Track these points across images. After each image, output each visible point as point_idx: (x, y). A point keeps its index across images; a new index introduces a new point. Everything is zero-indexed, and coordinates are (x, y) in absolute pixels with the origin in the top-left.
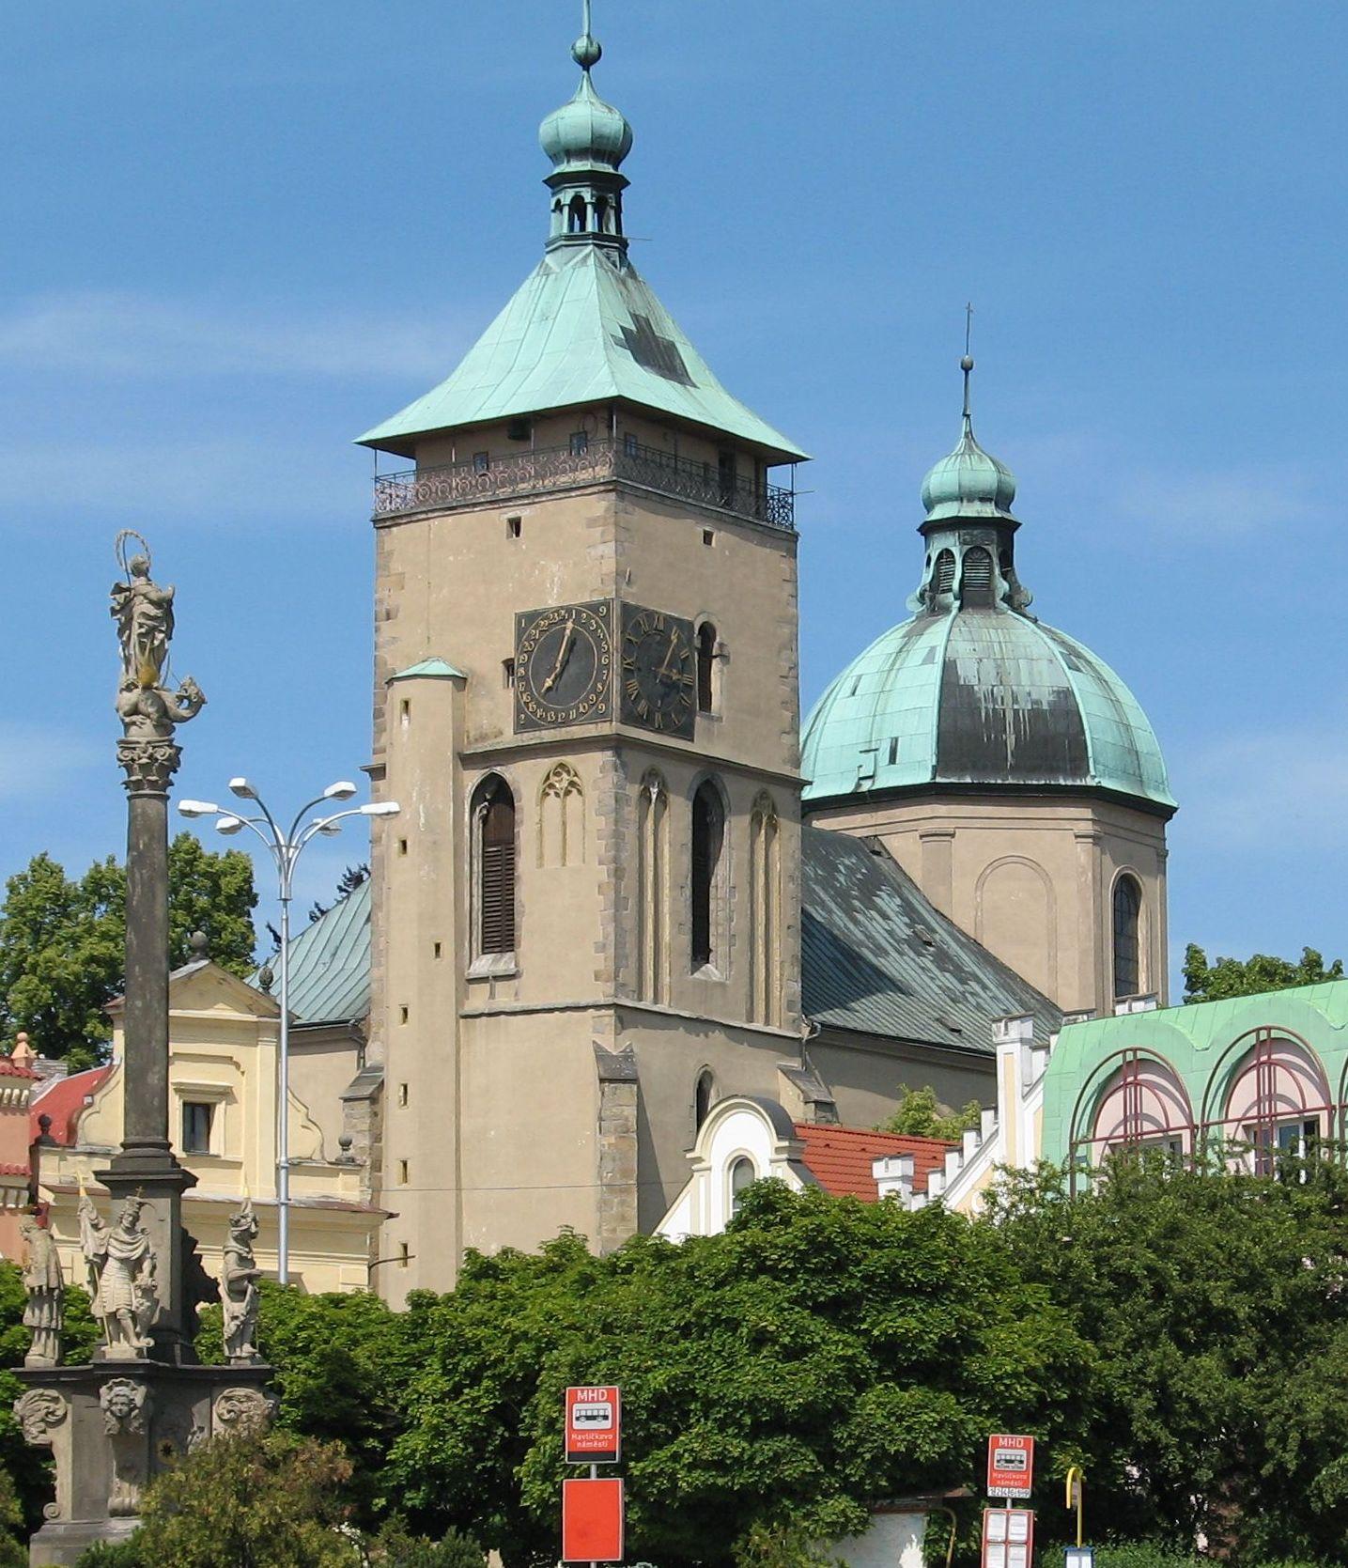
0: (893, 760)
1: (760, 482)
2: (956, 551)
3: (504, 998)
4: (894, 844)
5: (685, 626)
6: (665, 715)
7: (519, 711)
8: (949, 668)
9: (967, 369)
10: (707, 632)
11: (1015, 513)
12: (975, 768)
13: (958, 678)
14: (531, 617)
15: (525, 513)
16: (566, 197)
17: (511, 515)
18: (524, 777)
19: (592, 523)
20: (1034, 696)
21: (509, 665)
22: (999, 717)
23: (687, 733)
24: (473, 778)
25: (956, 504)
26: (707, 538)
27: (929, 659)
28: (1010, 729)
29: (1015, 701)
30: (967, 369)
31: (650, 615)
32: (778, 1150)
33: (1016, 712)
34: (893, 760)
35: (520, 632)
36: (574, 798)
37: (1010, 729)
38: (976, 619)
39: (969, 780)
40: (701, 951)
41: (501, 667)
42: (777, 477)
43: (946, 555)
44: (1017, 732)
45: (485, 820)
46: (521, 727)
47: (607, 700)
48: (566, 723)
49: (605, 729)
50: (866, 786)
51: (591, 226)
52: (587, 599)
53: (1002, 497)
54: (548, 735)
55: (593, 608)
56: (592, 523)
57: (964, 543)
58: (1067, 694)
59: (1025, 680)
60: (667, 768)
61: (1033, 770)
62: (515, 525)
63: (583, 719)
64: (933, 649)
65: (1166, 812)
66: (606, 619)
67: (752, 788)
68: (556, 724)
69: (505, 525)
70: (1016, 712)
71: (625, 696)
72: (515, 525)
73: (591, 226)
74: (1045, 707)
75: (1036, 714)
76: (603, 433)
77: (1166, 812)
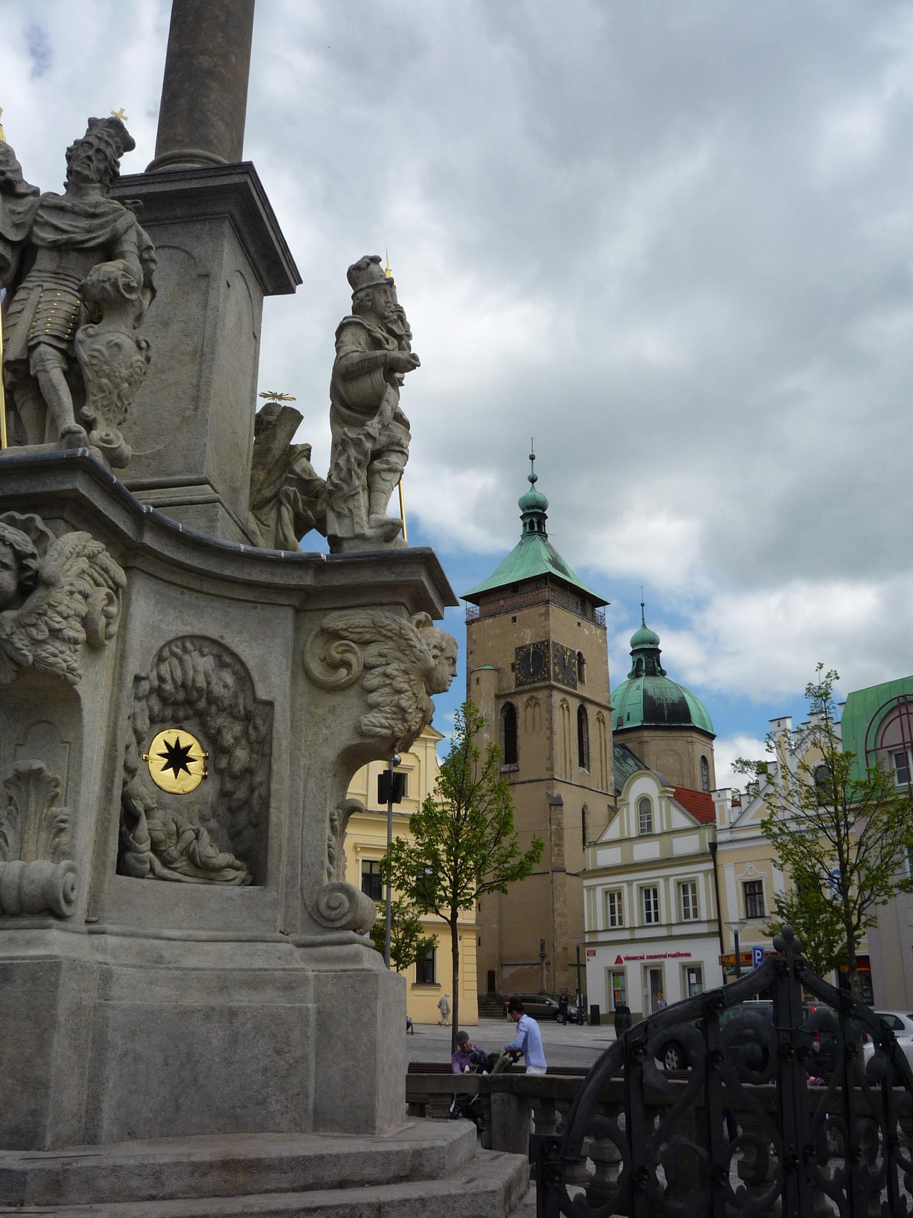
0: (628, 719)
1: (593, 611)
3: (513, 777)
4: (630, 746)
5: (573, 652)
6: (568, 681)
7: (517, 679)
8: (645, 691)
10: (580, 654)
11: (660, 647)
12: (654, 721)
14: (521, 648)
15: (517, 614)
16: (528, 521)
17: (513, 615)
18: (520, 702)
19: (541, 615)
21: (513, 665)
22: (661, 705)
23: (575, 687)
24: (502, 703)
26: (579, 624)
27: (638, 688)
31: (562, 647)
32: (662, 792)
34: (628, 719)
35: (517, 653)
36: (537, 709)
38: (651, 678)
40: (582, 764)
41: (510, 666)
42: (599, 610)
43: (640, 661)
45: (506, 719)
46: (517, 685)
47: (548, 673)
48: (534, 682)
49: (547, 683)
50: (620, 728)
51: (536, 529)
52: (540, 640)
54: (526, 687)
55: (542, 643)
56: (541, 615)
58: (683, 698)
60: (570, 699)
61: (673, 722)
62: (514, 619)
63: (540, 680)
65: (712, 737)
66: (548, 646)
67: (597, 709)
68: (530, 683)
69: (511, 620)
71: (554, 672)
72: (514, 619)
73: (536, 529)
75: (673, 704)
76: (543, 585)
77: (712, 737)
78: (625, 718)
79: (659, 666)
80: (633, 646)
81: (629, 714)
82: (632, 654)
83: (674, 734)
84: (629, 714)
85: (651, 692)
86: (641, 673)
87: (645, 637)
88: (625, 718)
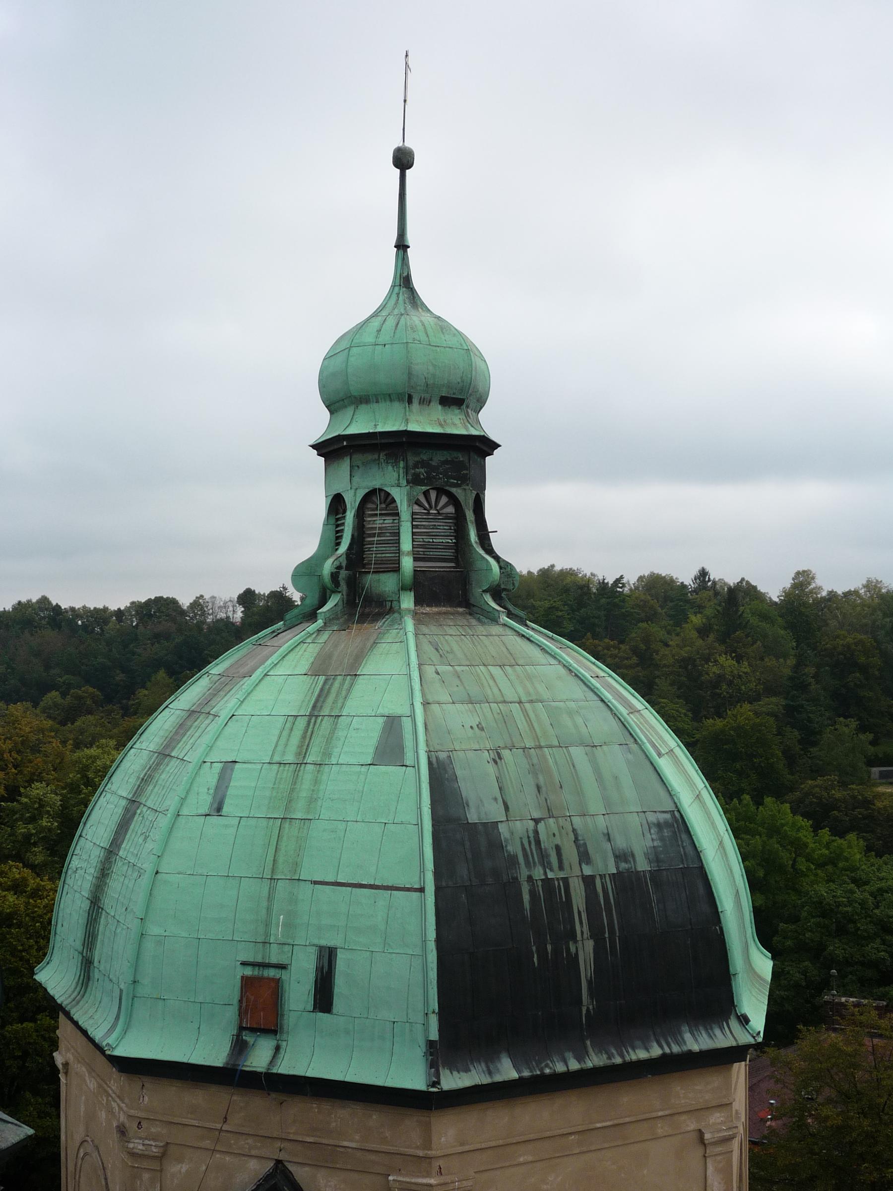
0: (323, 999)
2: (400, 495)
8: (441, 779)
9: (403, 160)
11: (490, 421)
13: (464, 805)
20: (620, 842)
22: (553, 895)
25: (398, 407)
27: (390, 749)
28: (582, 928)
29: (584, 857)
30: (403, 160)
33: (589, 881)
34: (323, 999)
37: (582, 928)
38: (456, 636)
39: (507, 1071)
43: (377, 500)
44: (596, 934)
53: (463, 396)
57: (414, 481)
59: (595, 806)
64: (392, 724)
70: (589, 881)
74: (642, 865)
75: (627, 882)
78: (298, 991)
79: (490, 551)
80: (337, 400)
81: (327, 960)
82: (330, 450)
83: (629, 1101)
84: (327, 960)
85: (481, 804)
86: (387, 583)
87: (422, 363)
88: (298, 991)
